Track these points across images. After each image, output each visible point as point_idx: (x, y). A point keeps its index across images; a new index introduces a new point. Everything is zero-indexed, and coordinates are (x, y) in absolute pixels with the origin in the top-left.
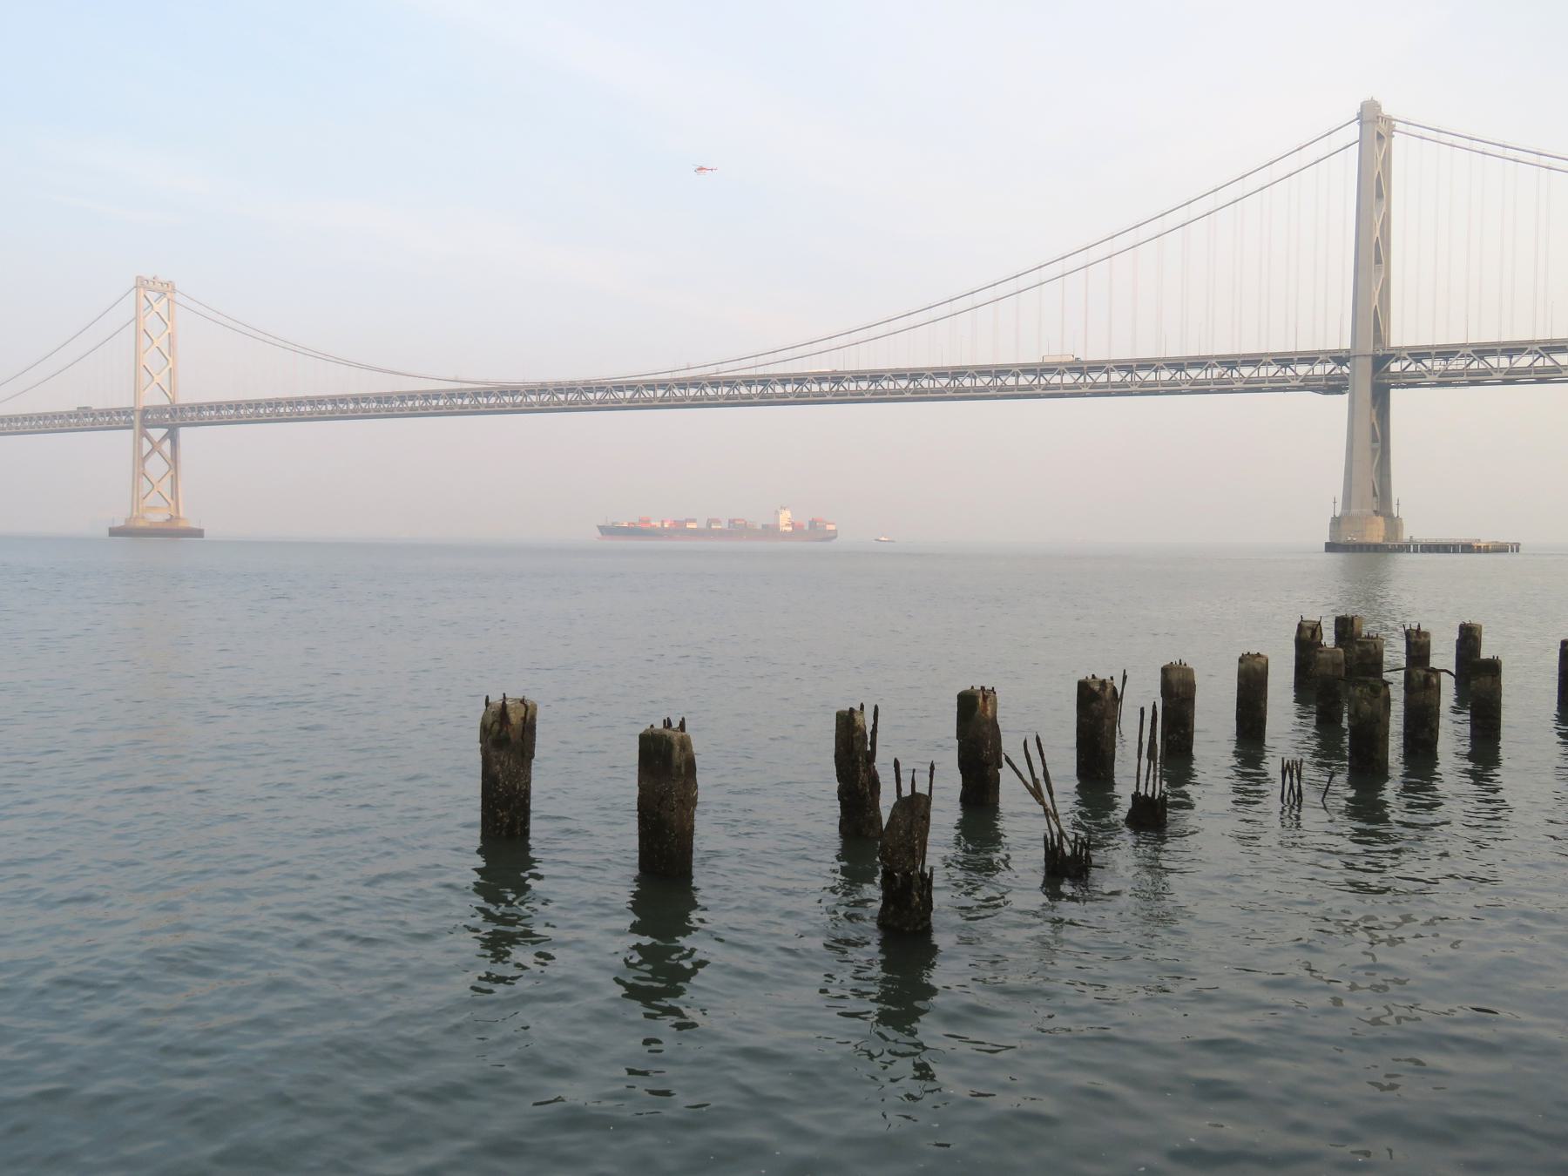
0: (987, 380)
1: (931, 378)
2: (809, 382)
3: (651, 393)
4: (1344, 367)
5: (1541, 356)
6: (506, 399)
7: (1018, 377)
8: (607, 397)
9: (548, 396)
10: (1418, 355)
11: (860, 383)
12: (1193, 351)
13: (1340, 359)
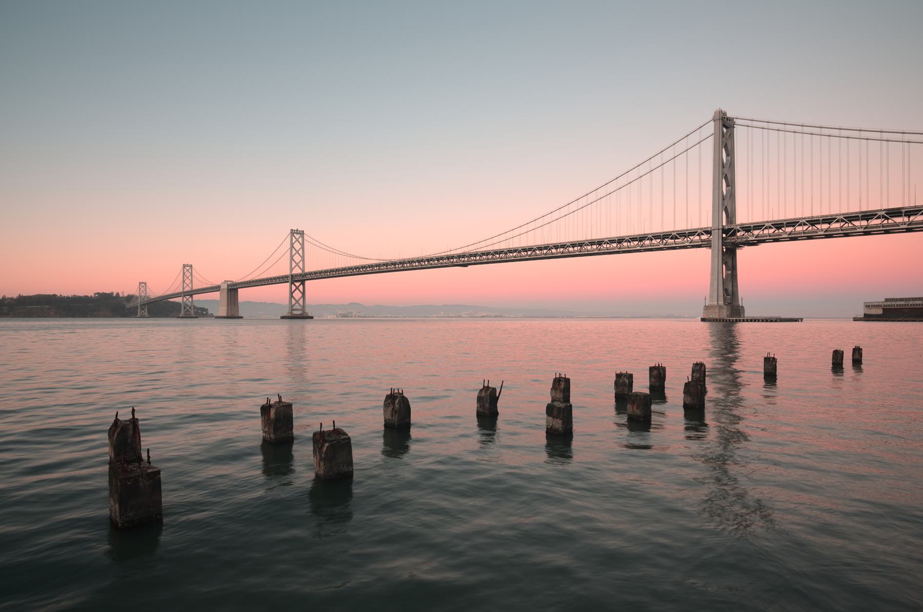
1: (608, 243)
2: (585, 245)
3: (526, 253)
4: (814, 227)
5: (846, 222)
10: (747, 229)
11: (593, 246)
13: (708, 232)
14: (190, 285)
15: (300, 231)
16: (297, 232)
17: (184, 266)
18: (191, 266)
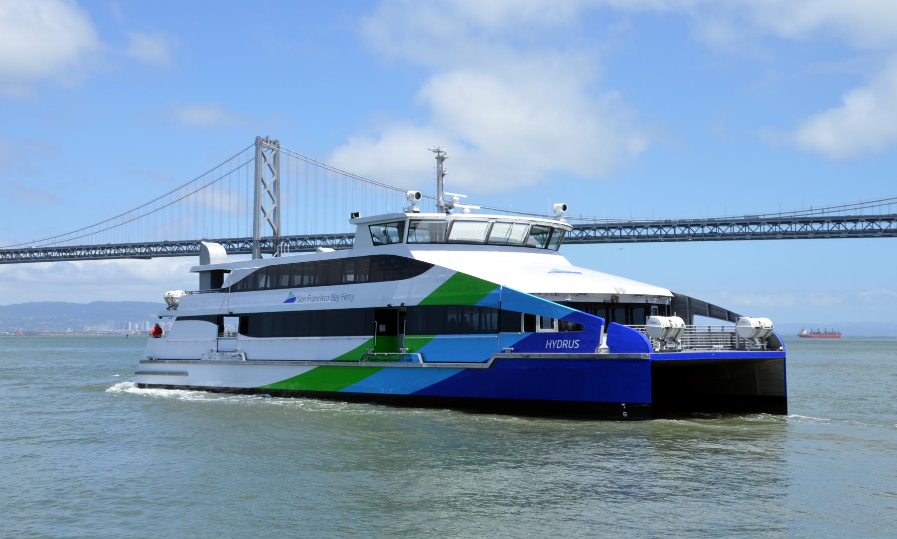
0: (602, 231)
6: (152, 248)
7: (621, 230)
8: (245, 246)
9: (193, 246)
12: (184, 238)
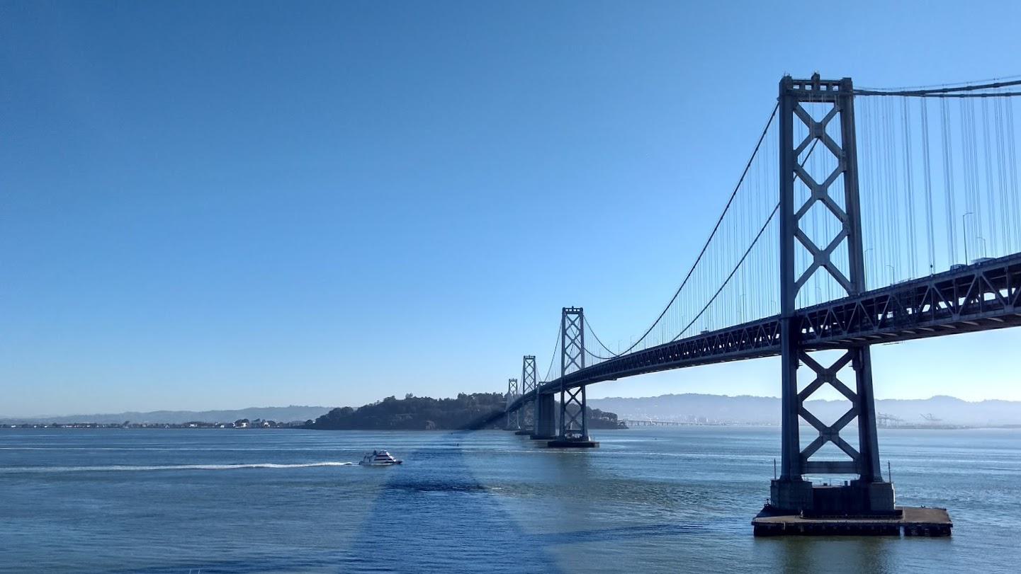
14: (578, 361)
15: (829, 84)
16: (816, 88)
17: (565, 312)
18: (580, 312)
